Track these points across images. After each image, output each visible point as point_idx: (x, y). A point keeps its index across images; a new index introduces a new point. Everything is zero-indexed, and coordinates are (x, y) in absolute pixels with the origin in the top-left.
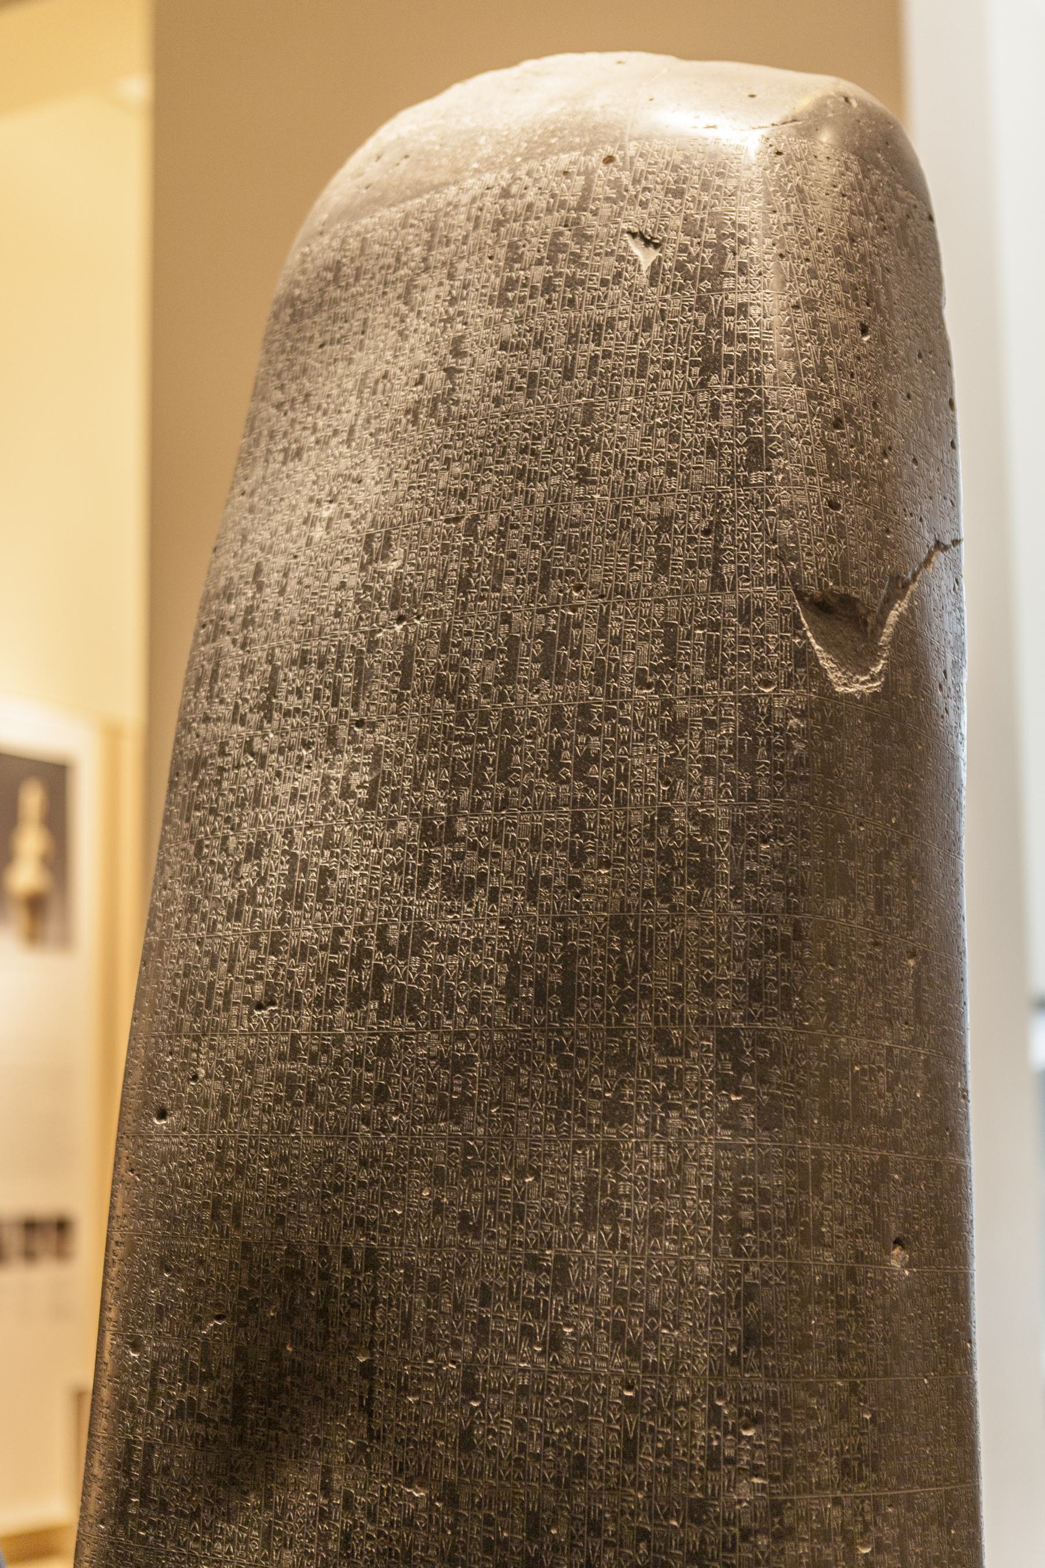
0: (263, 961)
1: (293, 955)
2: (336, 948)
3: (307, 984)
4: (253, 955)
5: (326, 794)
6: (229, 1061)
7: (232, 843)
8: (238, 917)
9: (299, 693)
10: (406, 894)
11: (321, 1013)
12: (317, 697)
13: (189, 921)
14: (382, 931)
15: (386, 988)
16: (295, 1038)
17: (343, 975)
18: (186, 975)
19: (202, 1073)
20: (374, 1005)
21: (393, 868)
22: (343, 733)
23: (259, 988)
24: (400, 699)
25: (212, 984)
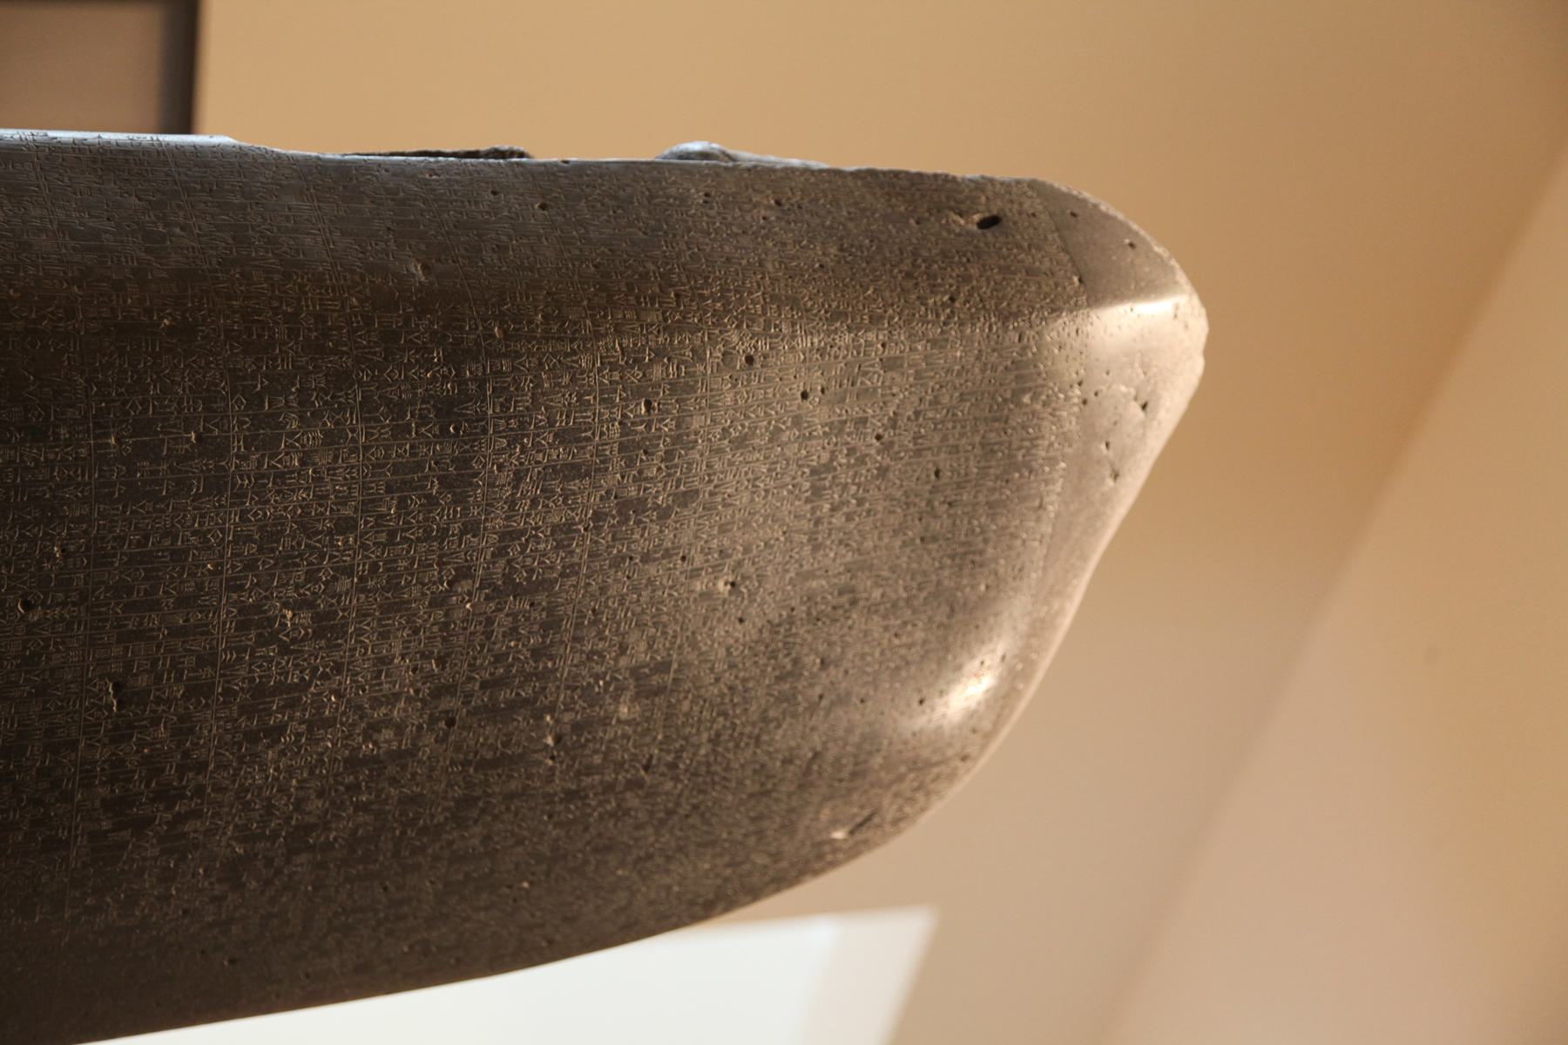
0: (179, 679)
1: (181, 719)
2: (182, 770)
3: (141, 744)
4: (189, 661)
5: (376, 703)
6: (49, 659)
7: (344, 584)
8: (243, 626)
9: (513, 632)
10: (236, 826)
11: (103, 769)
12: (499, 658)
13: (249, 539)
14: (197, 814)
15: (127, 834)
16: (73, 745)
17: (148, 786)
18: (173, 553)
19: (34, 617)
20: (106, 825)
21: (269, 808)
22: (447, 703)
23: (143, 681)
24: (466, 763)
25: (155, 606)
